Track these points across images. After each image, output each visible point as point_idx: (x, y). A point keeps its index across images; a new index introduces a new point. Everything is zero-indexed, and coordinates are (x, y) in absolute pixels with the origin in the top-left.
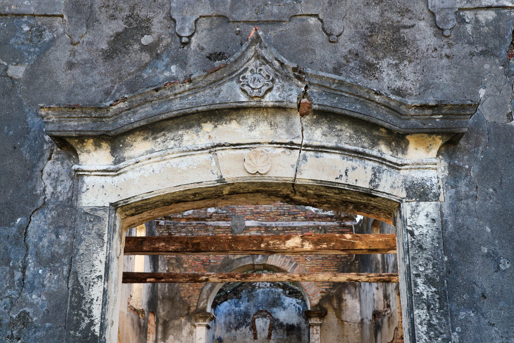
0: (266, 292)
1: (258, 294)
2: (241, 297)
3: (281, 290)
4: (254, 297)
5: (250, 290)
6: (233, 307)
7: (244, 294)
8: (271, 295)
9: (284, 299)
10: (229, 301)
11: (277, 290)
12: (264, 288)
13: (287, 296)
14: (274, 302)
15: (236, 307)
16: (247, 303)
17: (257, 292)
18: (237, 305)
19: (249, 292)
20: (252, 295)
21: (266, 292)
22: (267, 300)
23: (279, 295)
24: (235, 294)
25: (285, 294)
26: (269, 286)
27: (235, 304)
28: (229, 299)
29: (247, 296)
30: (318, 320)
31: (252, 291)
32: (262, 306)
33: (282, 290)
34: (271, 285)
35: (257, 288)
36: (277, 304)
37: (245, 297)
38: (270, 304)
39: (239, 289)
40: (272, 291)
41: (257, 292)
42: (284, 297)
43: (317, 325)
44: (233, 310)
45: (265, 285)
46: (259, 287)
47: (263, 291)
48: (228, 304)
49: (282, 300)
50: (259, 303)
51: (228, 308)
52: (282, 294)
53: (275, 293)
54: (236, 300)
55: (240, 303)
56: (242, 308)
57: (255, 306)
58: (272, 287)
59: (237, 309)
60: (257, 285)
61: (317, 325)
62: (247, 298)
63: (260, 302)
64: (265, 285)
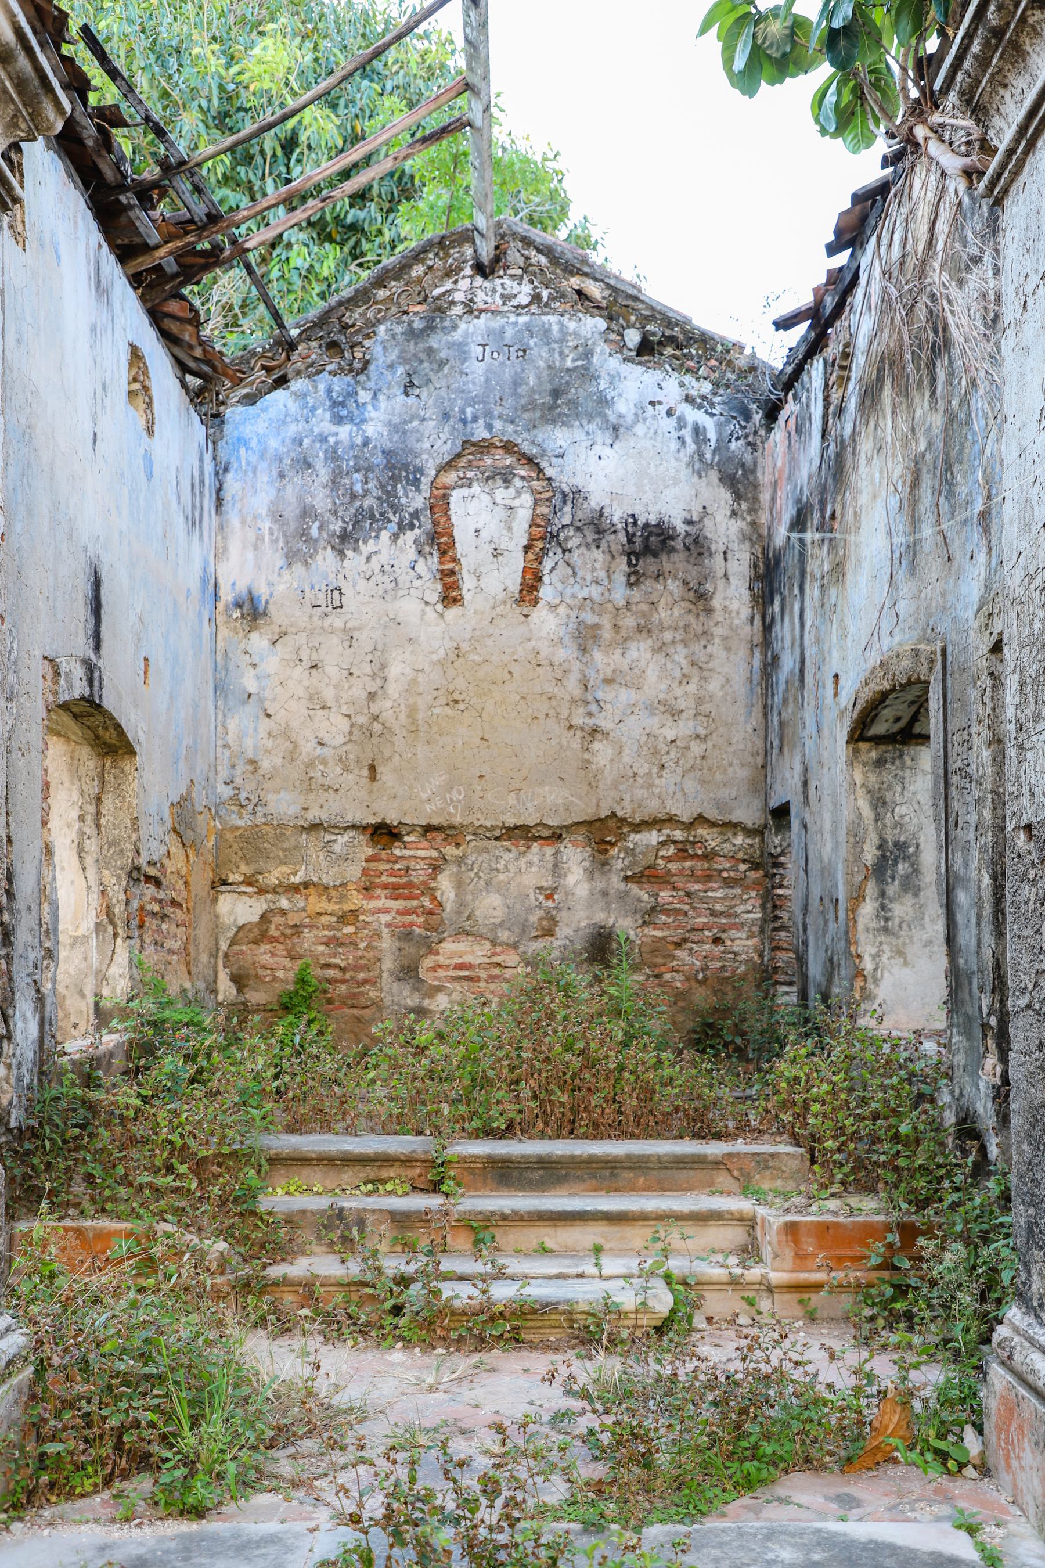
1: (461, 349)
2: (366, 363)
4: (442, 364)
5: (418, 324)
6: (322, 421)
7: (383, 347)
9: (614, 379)
10: (297, 385)
11: (572, 326)
14: (556, 393)
15: (339, 420)
17: (457, 336)
18: (341, 409)
19: (412, 334)
20: (430, 351)
23: (588, 354)
24: (333, 346)
26: (525, 300)
27: (335, 404)
28: (298, 373)
29: (403, 359)
31: (430, 328)
32: (488, 414)
33: (601, 324)
34: (536, 298)
35: (458, 310)
36: (573, 404)
37: (391, 367)
38: (530, 406)
39: (355, 316)
40: (546, 332)
41: (457, 336)
42: (614, 363)
44: (324, 439)
45: (506, 298)
46: (470, 308)
48: (293, 406)
49: (603, 385)
50: (472, 402)
51: (293, 429)
52: (601, 349)
53: (562, 340)
54: (339, 384)
55: (364, 396)
56: (370, 430)
57: (446, 416)
59: (344, 431)
60: (459, 296)
62: (400, 370)
63: (475, 390)
64: (506, 298)
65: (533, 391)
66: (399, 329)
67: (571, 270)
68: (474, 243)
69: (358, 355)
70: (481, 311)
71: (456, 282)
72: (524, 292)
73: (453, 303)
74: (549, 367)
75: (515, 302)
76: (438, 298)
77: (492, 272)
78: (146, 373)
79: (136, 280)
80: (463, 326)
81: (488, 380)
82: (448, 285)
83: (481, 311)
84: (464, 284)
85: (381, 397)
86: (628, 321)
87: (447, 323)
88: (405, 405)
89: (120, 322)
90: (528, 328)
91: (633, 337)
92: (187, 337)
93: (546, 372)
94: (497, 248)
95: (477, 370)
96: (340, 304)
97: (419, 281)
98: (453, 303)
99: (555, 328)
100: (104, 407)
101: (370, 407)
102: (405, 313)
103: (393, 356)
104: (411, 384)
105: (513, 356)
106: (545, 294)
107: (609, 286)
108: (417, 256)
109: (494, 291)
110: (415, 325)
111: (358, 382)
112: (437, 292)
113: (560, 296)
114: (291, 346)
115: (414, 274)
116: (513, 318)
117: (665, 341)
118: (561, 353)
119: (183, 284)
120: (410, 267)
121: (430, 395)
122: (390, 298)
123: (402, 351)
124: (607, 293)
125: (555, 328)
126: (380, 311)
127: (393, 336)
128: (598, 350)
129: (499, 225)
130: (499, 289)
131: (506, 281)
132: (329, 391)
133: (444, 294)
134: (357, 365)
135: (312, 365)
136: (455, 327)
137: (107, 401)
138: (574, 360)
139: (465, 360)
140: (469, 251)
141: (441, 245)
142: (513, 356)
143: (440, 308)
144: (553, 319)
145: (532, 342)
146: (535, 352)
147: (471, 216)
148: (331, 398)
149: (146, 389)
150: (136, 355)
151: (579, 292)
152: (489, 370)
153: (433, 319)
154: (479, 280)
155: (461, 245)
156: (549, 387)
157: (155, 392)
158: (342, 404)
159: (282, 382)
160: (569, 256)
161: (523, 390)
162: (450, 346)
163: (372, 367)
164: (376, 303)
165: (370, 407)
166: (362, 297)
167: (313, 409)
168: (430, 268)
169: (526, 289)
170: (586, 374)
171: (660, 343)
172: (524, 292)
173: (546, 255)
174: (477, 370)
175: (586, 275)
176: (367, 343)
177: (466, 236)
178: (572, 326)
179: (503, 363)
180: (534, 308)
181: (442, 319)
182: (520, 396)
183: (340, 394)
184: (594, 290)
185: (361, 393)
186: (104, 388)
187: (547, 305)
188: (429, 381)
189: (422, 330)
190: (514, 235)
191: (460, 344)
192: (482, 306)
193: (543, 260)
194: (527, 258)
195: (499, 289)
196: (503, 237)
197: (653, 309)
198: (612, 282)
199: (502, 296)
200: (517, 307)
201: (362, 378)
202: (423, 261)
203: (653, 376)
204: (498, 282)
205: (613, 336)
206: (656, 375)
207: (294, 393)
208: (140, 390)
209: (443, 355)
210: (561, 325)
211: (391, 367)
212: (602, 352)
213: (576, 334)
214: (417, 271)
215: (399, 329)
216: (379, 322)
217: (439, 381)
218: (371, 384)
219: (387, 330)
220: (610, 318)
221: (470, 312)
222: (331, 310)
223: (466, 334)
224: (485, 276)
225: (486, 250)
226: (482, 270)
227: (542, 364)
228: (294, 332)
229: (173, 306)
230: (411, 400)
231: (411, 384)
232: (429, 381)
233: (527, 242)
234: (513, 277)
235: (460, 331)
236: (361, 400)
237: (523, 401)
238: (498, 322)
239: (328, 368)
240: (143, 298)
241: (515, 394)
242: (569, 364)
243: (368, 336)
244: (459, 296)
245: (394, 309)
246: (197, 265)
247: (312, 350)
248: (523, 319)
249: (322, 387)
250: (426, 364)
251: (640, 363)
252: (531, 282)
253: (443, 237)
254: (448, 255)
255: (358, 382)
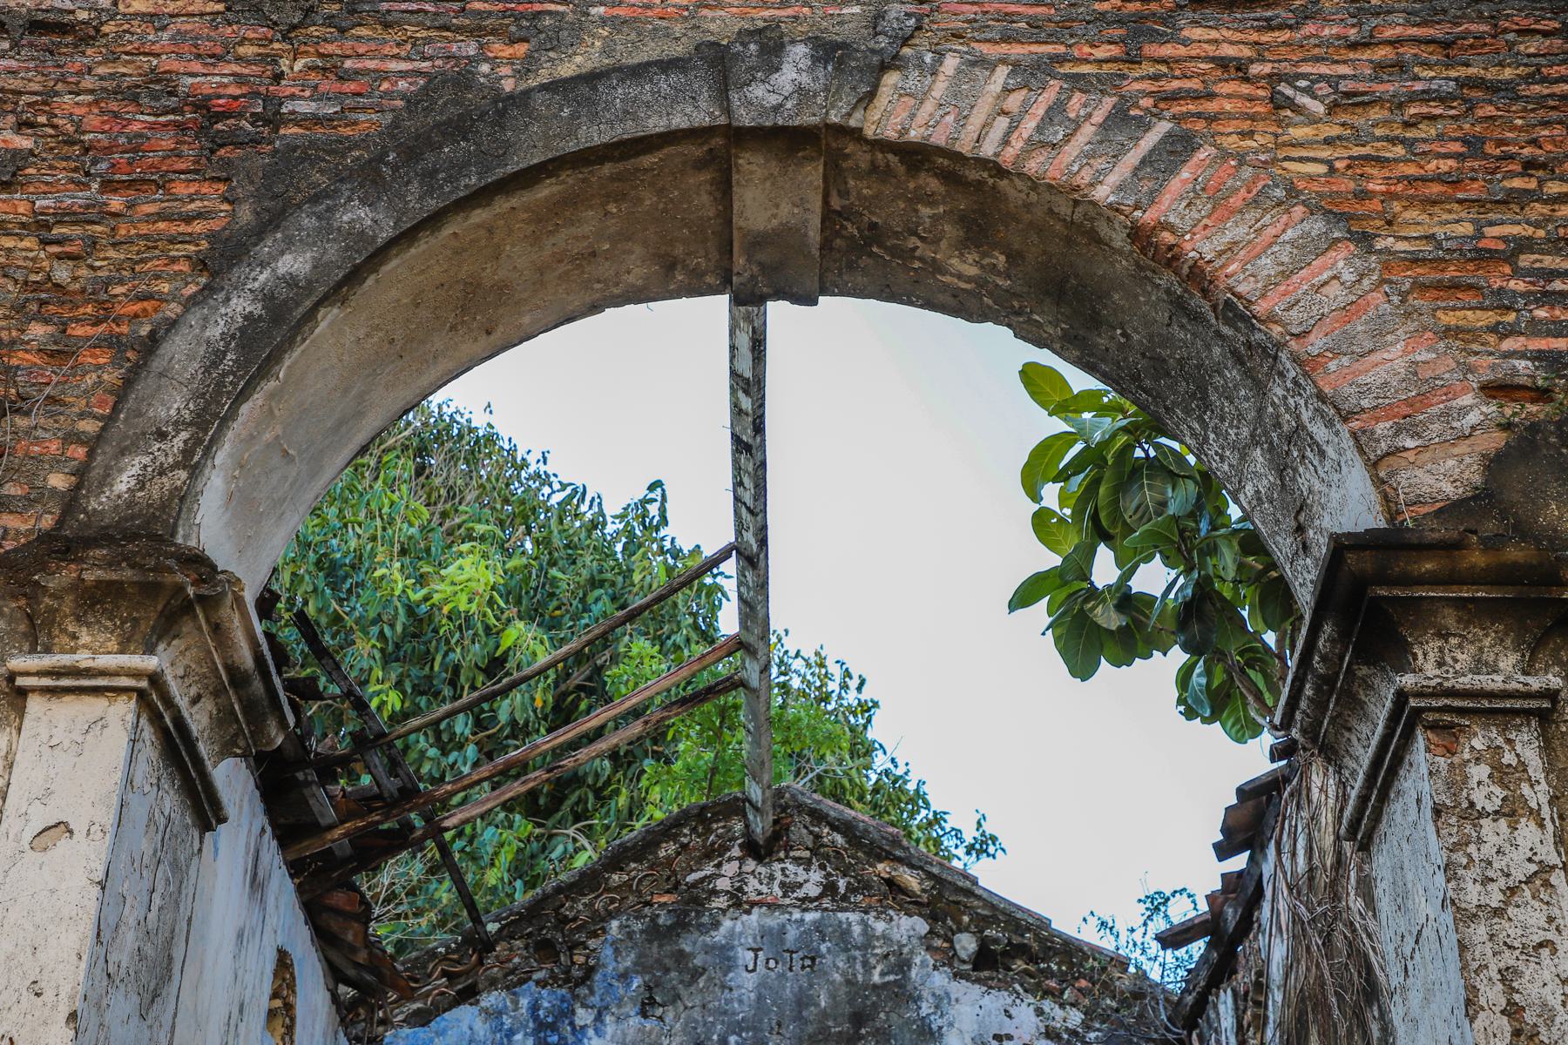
0: (792, 934)
1: (725, 957)
2: (590, 971)
3: (908, 927)
4: (696, 973)
7: (613, 949)
8: (836, 966)
9: (940, 1001)
10: (491, 999)
11: (880, 926)
12: (772, 907)
13: (958, 975)
14: (858, 1019)
16: (635, 1021)
17: (719, 936)
19: (655, 933)
20: (681, 956)
21: (792, 934)
22: (803, 1001)
23: (903, 965)
24: (546, 950)
25: (948, 958)
26: (813, 890)
27: (541, 1026)
28: (493, 983)
29: (641, 967)
30: (1508, 662)
31: (681, 925)
33: (922, 926)
34: (829, 888)
35: (721, 902)
37: (624, 976)
39: (579, 907)
40: (844, 933)
41: (719, 936)
42: (940, 980)
43: (1499, 710)
46: (738, 901)
47: (765, 933)
48: (482, 1029)
49: (926, 1009)
52: (921, 957)
53: (867, 946)
55: (583, 1016)
58: (843, 902)
60: (723, 884)
61: (1499, 710)
62: (636, 982)
63: (742, 1012)
65: (824, 1014)
66: (637, 926)
67: (878, 853)
68: (745, 816)
69: (580, 959)
70: (753, 904)
71: (719, 866)
72: (812, 881)
73: (715, 893)
74: (848, 982)
75: (800, 894)
76: (695, 885)
77: (770, 853)
78: (292, 987)
79: (295, 868)
80: (727, 923)
81: (760, 998)
82: (709, 870)
83: (753, 904)
84: (730, 869)
85: (608, 1019)
86: (959, 922)
87: (705, 919)
88: (641, 1030)
89: (272, 921)
90: (818, 927)
91: (967, 944)
92: (350, 937)
93: (843, 990)
94: (776, 822)
95: (746, 983)
96: (559, 890)
97: (669, 861)
98: (715, 893)
99: (857, 929)
100: (237, 1035)
101: (591, 1032)
102: (649, 904)
103: (628, 962)
104: (652, 1002)
105: (797, 967)
106: (842, 884)
107: (930, 875)
108: (668, 830)
109: (772, 878)
110: (661, 921)
111: (576, 997)
112: (691, 878)
113: (864, 886)
114: (485, 945)
115: (662, 853)
116: (797, 915)
117: (1015, 950)
118: (865, 964)
119: (357, 871)
120: (657, 845)
121: (677, 1018)
122: (627, 885)
123: (639, 956)
124: (928, 884)
125: (857, 929)
126: (613, 901)
127: (630, 935)
128: (917, 960)
129: (779, 793)
130: (778, 875)
131: (791, 867)
132: (534, 1007)
133: (702, 880)
134: (576, 973)
135: (512, 972)
136: (716, 925)
137: (242, 1027)
138: (882, 974)
139: (729, 969)
140: (738, 827)
141: (699, 817)
142: (797, 967)
143: (695, 900)
144: (853, 917)
145: (823, 948)
146: (828, 960)
147: (742, 783)
148: (536, 1018)
149: (289, 1007)
150: (283, 962)
151: (890, 882)
152: (762, 985)
153: (686, 914)
154: (751, 865)
155: (727, 818)
156: (848, 1010)
157: (300, 1012)
158: (553, 1027)
159: (469, 995)
160: (876, 836)
161: (810, 1013)
162: (708, 949)
163: (598, 977)
164: (607, 890)
165: (591, 1032)
166: (590, 880)
167: (511, 1033)
168: (684, 847)
169: (816, 876)
170: (901, 992)
171: (1004, 953)
172: (812, 881)
173: (844, 834)
174: (746, 983)
175: (899, 860)
176: (592, 943)
177: (736, 807)
178: (880, 926)
179: (782, 976)
180: (826, 903)
181: (699, 914)
182: (806, 1022)
183: (549, 1012)
184: (911, 879)
185: (580, 1012)
186: (241, 1011)
187: (845, 898)
188: (678, 997)
189: (670, 928)
190: (800, 807)
191: (723, 947)
192: (753, 897)
193: (839, 839)
194: (817, 837)
195: (778, 875)
196: (785, 808)
197: (993, 907)
198: (935, 870)
199: (783, 885)
200: (803, 900)
201: (583, 991)
202: (675, 838)
203: (996, 1001)
204: (777, 866)
205: (938, 943)
206: (1001, 999)
207: (485, 1011)
208: (282, 1013)
209: (698, 962)
210: (864, 923)
211: (624, 976)
212: (924, 964)
213: (885, 938)
214: (667, 850)
215: (637, 926)
216: (611, 915)
217: (692, 999)
218: (595, 1000)
219: (621, 927)
220: (933, 918)
221: (737, 904)
222: (546, 897)
223: (731, 933)
224: (760, 859)
225: (761, 826)
226: (757, 850)
227: (837, 977)
228: (492, 927)
229: (339, 899)
230: (649, 1025)
231: (652, 1002)
232: (678, 997)
233: (818, 816)
234: (797, 861)
235: (722, 930)
236: (579, 1022)
237: (810, 1029)
238: (775, 920)
239: (535, 976)
240: (300, 889)
241: (799, 1018)
242: (876, 978)
243: (594, 935)
244: (723, 884)
245: (632, 899)
246: (373, 850)
247: (516, 952)
248: (810, 917)
249: (524, 1002)
250: (673, 974)
251: (978, 981)
252: (822, 867)
253: (704, 808)
254: (709, 831)
255: (576, 997)
